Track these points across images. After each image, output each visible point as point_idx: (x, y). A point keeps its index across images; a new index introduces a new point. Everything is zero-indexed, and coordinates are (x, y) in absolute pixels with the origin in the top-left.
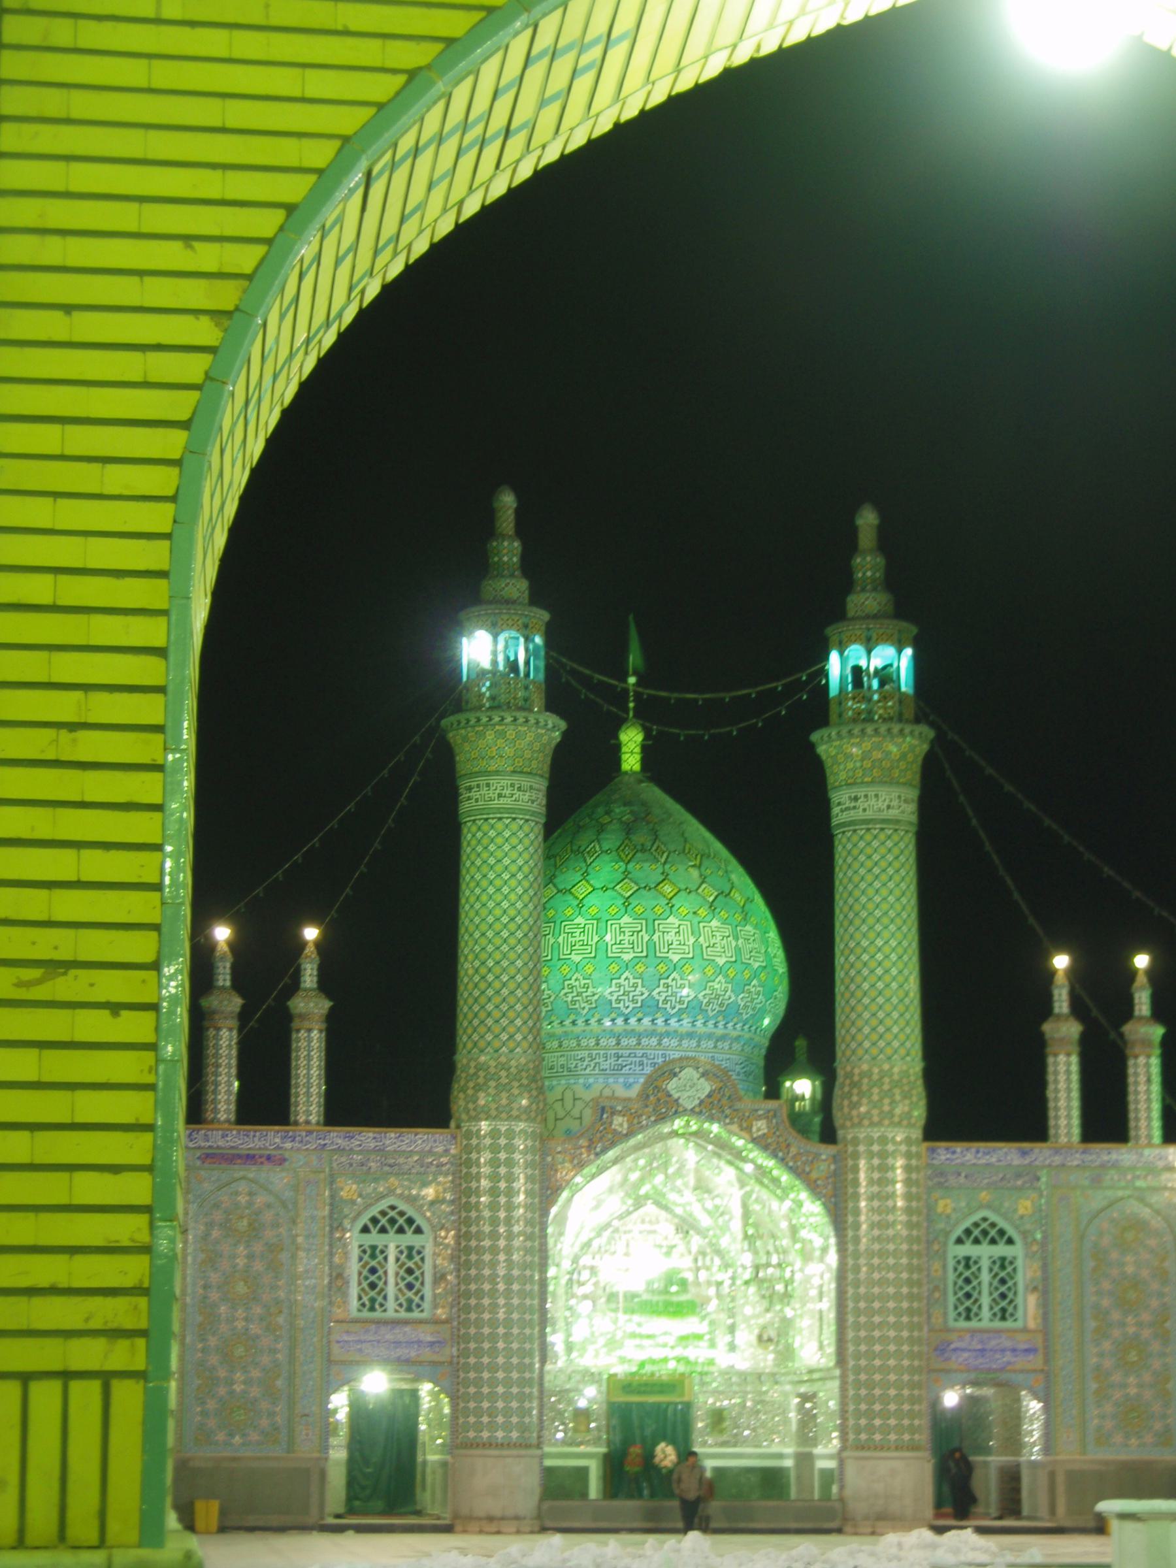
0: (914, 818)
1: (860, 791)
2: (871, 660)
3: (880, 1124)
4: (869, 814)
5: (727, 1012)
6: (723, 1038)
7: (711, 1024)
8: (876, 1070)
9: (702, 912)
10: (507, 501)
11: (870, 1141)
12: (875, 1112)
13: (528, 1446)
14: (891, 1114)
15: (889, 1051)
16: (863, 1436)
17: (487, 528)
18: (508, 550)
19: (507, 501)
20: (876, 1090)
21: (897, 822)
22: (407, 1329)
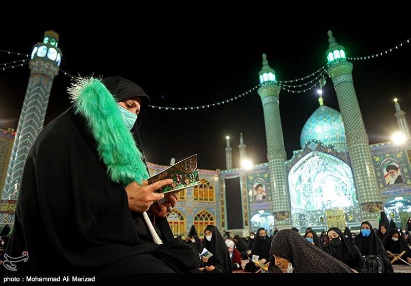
0: (352, 80)
1: (337, 78)
2: (336, 55)
3: (355, 143)
4: (340, 82)
5: (341, 138)
6: (342, 143)
7: (338, 141)
8: (352, 132)
9: (332, 121)
10: (264, 56)
11: (354, 148)
12: (353, 141)
13: (289, 224)
14: (357, 141)
15: (354, 127)
16: (366, 216)
17: (262, 60)
18: (265, 62)
19: (264, 56)
20: (353, 136)
21: (346, 82)
22: (263, 203)
